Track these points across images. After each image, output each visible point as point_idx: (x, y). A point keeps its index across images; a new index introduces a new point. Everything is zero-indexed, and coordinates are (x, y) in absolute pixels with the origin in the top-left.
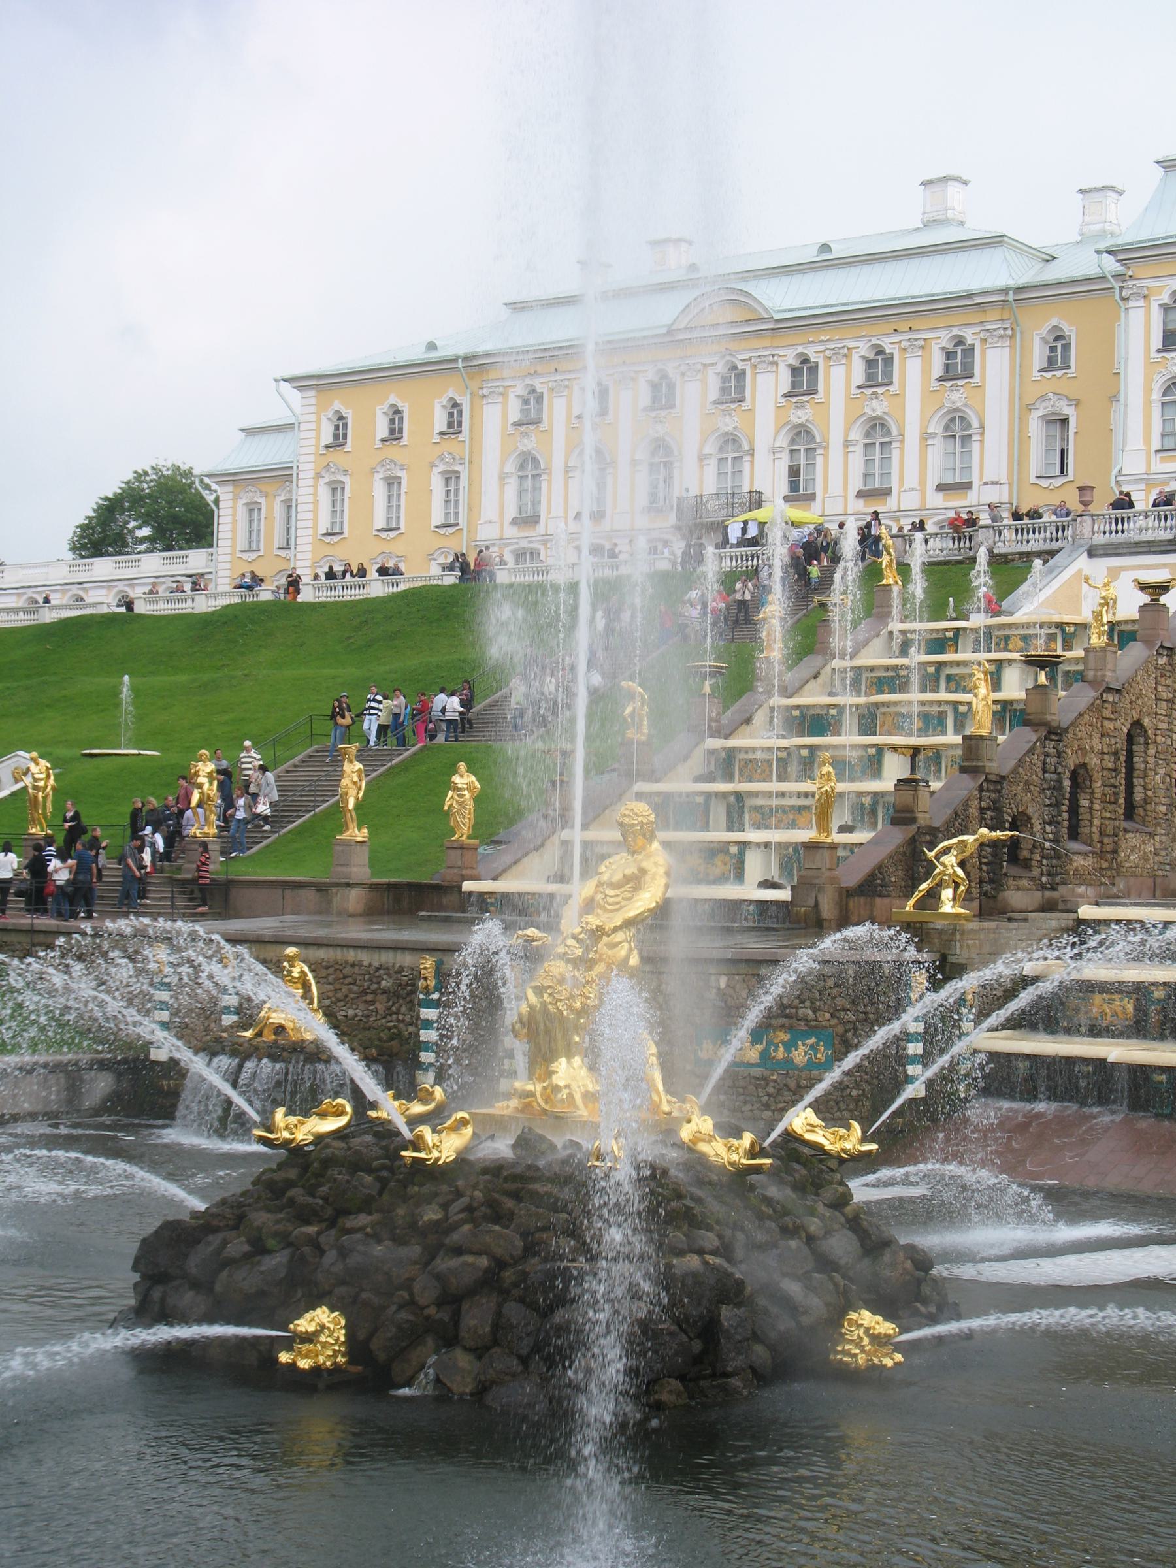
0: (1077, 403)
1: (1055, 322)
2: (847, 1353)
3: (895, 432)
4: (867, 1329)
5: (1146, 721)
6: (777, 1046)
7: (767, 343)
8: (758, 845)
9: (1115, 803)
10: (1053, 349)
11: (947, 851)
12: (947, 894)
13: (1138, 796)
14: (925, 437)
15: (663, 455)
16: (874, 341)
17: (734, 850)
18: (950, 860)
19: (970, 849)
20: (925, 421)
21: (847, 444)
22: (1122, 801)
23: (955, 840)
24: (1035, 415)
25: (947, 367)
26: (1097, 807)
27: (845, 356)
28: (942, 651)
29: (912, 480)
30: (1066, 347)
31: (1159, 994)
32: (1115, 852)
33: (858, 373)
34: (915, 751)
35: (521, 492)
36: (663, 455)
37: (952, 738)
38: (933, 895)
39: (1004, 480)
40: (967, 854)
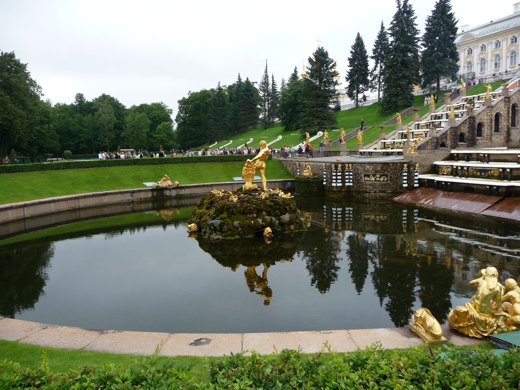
5: (501, 112)
14: (507, 57)
20: (507, 54)
29: (504, 67)
32: (491, 139)
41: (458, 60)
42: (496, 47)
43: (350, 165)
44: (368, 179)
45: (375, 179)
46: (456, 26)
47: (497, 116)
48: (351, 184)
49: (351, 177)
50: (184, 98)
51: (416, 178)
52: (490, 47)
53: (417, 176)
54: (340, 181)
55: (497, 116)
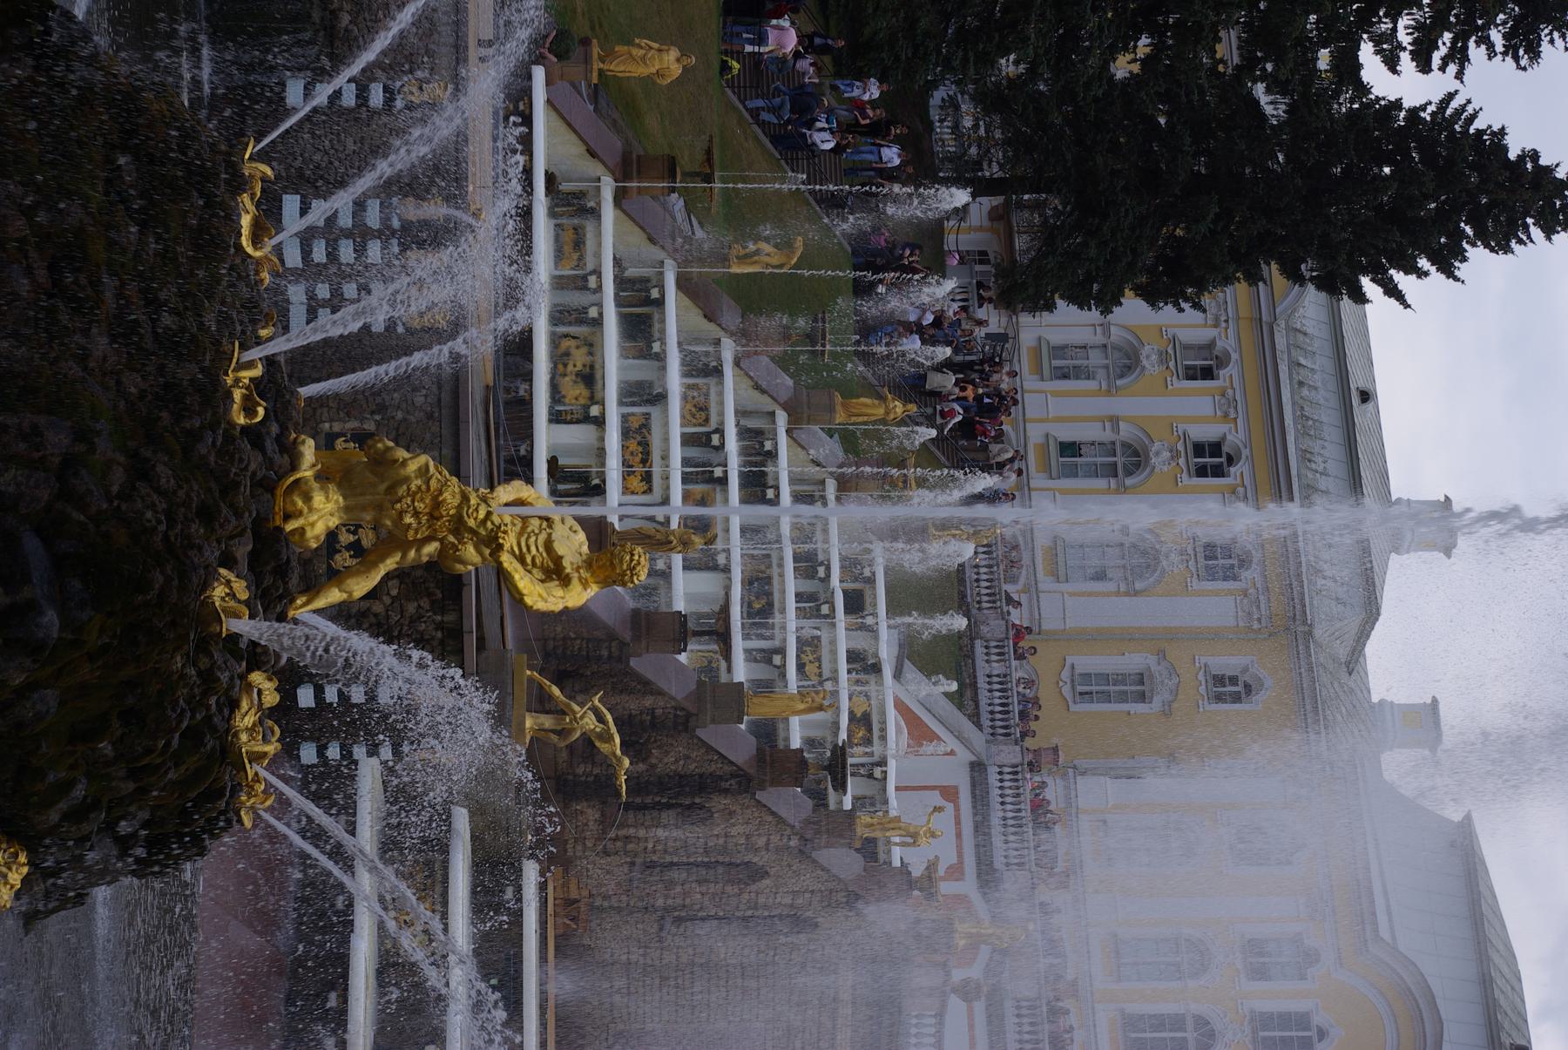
0: (1167, 711)
1: (1268, 683)
3: (1129, 482)
5: (767, 882)
7: (1244, 313)
8: (602, 439)
9: (666, 851)
10: (1234, 680)
11: (601, 719)
12: (547, 721)
13: (675, 874)
16: (1245, 452)
17: (595, 411)
18: (590, 722)
19: (604, 747)
21: (1115, 421)
23: (613, 729)
24: (1152, 661)
27: (1226, 415)
30: (1236, 698)
33: (1206, 432)
34: (724, 638)
37: (741, 672)
38: (542, 703)
39: (1070, 624)
40: (597, 744)
41: (1152, 296)
42: (1199, 449)
46: (1366, 283)
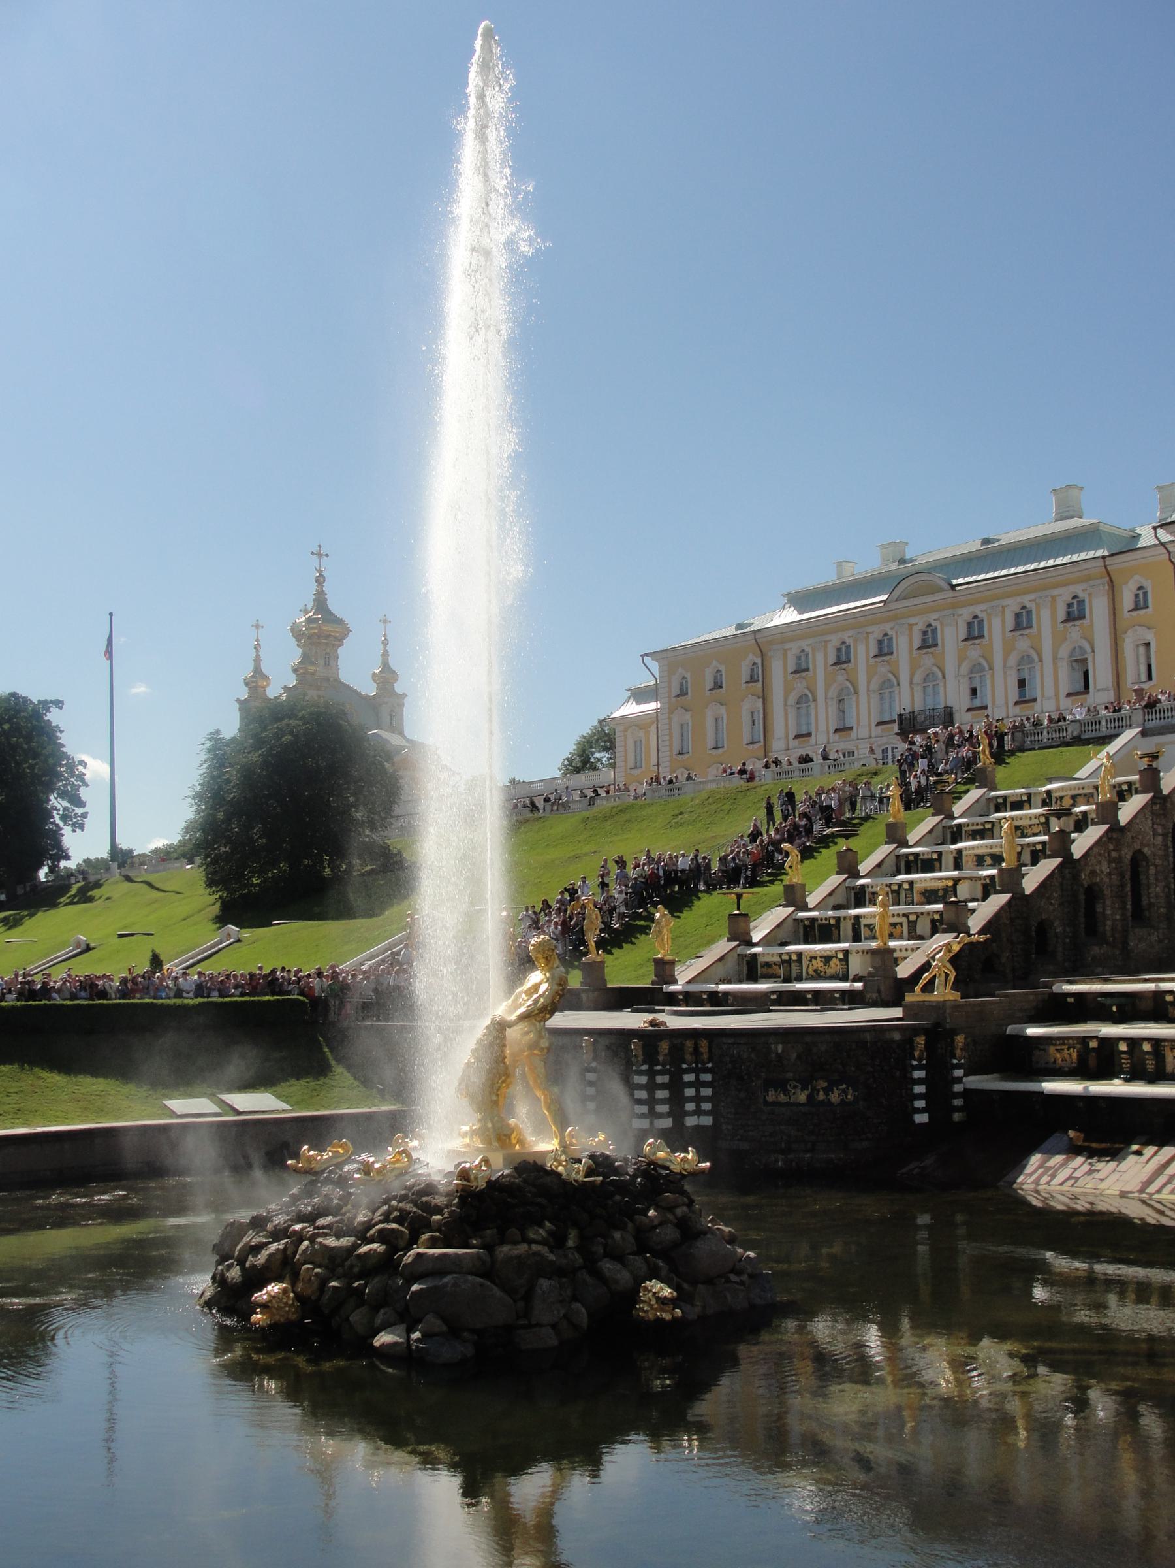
2: (642, 1310)
4: (654, 1293)
5: (1146, 850)
6: (818, 1091)
10: (1137, 596)
13: (1145, 902)
14: (1055, 658)
15: (887, 688)
17: (840, 956)
22: (1129, 907)
25: (1069, 613)
26: (1108, 912)
28: (1021, 808)
29: (1050, 691)
30: (1145, 594)
31: (1093, 1044)
32: (1125, 943)
33: (1010, 623)
35: (798, 716)
36: (887, 688)
38: (932, 981)
43: (704, 1043)
44: (782, 1098)
45: (809, 1097)
47: (1137, 860)
48: (707, 1121)
49: (707, 1092)
50: (215, 737)
51: (958, 1088)
52: (996, 623)
53: (959, 1080)
54: (664, 1108)
55: (1137, 860)
